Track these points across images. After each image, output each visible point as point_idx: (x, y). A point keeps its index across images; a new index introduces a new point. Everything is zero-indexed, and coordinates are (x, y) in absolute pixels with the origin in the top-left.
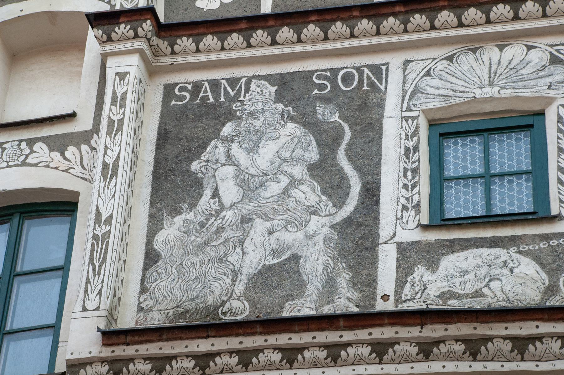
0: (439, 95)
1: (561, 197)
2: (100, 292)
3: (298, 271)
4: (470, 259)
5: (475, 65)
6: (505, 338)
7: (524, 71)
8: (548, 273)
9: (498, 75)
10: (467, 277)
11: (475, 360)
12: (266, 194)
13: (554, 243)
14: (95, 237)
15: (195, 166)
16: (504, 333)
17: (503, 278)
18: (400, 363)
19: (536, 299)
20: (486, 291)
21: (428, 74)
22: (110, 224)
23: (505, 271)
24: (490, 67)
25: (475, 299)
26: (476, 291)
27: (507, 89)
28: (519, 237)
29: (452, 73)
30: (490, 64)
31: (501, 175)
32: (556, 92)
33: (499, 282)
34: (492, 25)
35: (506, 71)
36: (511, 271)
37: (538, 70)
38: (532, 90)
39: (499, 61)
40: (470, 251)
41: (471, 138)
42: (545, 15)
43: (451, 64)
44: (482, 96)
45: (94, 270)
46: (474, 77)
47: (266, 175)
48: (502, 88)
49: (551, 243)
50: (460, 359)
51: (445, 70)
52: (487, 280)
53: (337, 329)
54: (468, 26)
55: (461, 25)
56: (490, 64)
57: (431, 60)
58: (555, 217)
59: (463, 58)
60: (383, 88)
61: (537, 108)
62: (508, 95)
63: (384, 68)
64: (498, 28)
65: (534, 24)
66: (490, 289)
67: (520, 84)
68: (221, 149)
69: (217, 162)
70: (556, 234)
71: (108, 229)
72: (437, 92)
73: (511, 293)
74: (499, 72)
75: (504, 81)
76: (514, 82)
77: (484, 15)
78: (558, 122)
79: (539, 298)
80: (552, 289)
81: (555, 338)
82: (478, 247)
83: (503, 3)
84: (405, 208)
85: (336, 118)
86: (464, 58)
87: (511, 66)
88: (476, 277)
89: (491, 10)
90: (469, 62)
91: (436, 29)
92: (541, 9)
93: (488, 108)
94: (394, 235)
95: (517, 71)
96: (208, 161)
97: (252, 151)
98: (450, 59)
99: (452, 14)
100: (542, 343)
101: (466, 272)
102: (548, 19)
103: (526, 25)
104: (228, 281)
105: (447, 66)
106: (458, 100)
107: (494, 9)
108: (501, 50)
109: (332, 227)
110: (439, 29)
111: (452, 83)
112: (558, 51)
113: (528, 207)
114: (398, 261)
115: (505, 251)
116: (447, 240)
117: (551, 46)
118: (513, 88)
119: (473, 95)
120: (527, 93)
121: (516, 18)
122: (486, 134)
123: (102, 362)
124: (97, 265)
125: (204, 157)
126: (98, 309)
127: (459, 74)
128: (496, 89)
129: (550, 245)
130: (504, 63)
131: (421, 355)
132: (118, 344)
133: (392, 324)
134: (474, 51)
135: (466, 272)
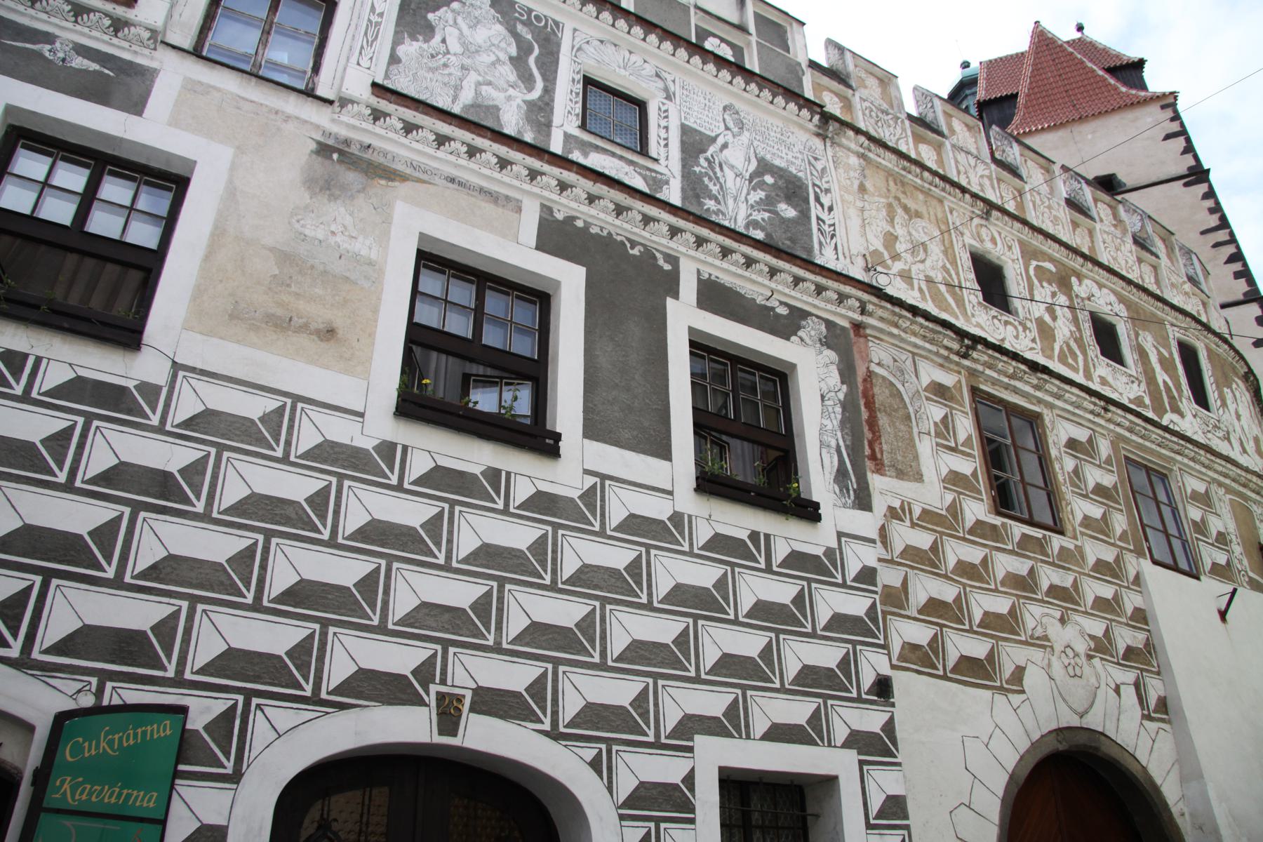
2: (371, 58)
3: (498, 117)
7: (642, 72)
11: (617, 218)
12: (481, 59)
13: (654, 174)
14: (369, 20)
15: (430, 16)
16: (641, 208)
18: (572, 200)
21: (588, 42)
22: (382, 17)
45: (368, 42)
47: (479, 47)
50: (609, 214)
53: (541, 160)
60: (560, 36)
63: (561, 25)
68: (450, 16)
69: (447, 22)
71: (380, 20)
84: (569, 112)
85: (529, 37)
94: (562, 125)
96: (440, 18)
97: (471, 27)
98: (602, 42)
104: (450, 100)
109: (524, 102)
114: (564, 142)
123: (367, 106)
124: (370, 40)
125: (437, 13)
126: (369, 69)
128: (627, 73)
131: (587, 201)
132: (384, 99)
133: (577, 173)
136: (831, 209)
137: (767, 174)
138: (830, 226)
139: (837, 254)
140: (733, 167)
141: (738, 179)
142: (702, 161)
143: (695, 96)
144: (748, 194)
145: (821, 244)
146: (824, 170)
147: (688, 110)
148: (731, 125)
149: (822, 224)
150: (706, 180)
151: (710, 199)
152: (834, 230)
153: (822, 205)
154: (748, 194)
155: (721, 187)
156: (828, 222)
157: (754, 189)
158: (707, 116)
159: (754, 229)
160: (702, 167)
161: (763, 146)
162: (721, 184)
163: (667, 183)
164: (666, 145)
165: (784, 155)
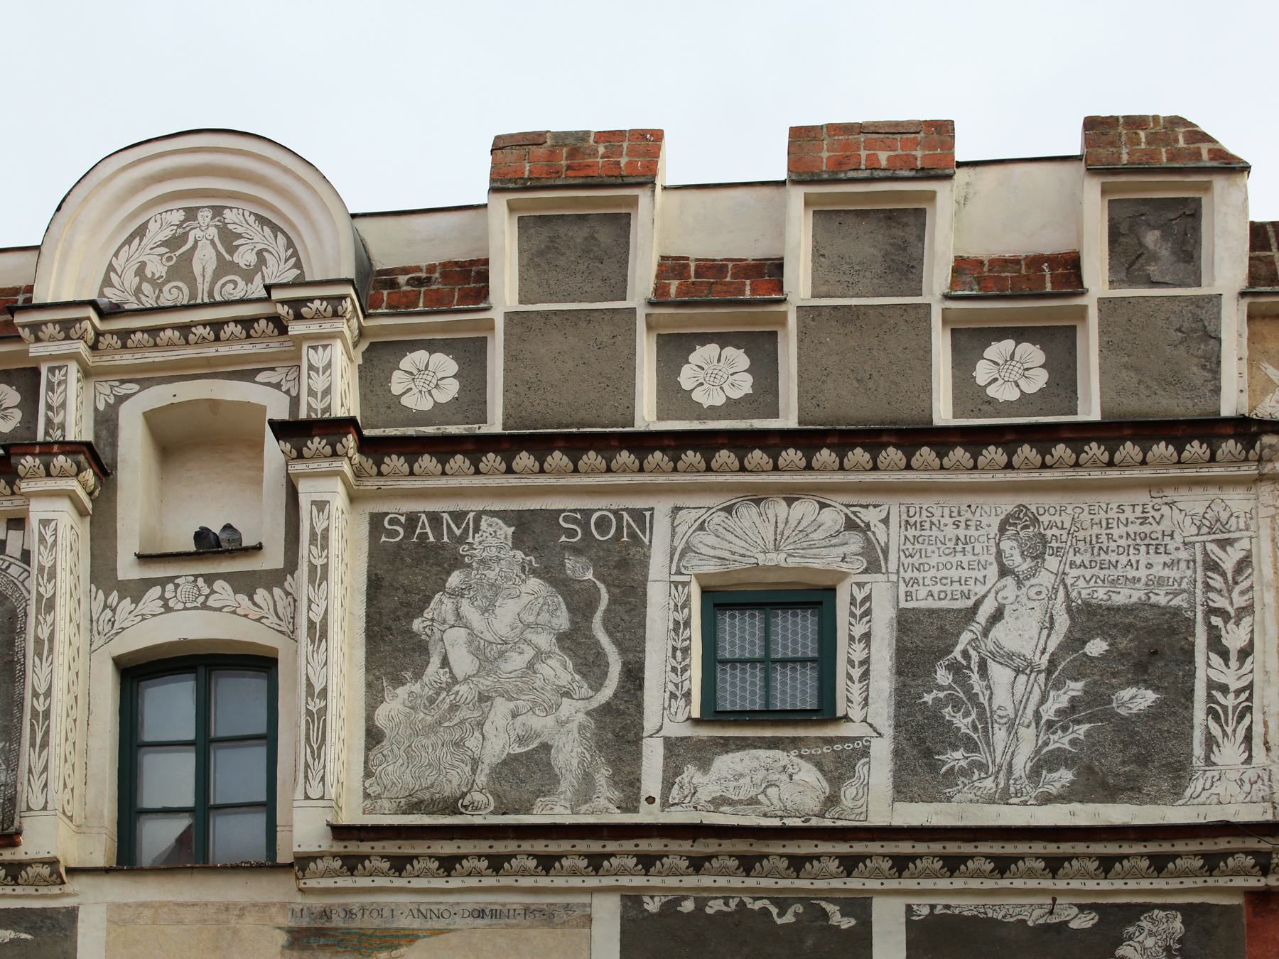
0: (715, 557)
1: (849, 695)
4: (746, 761)
5: (758, 521)
6: (781, 856)
8: (830, 781)
9: (785, 538)
10: (742, 781)
13: (838, 747)
17: (781, 785)
19: (815, 809)
20: (761, 798)
23: (784, 777)
24: (776, 527)
25: (749, 807)
26: (751, 798)
27: (795, 557)
28: (800, 739)
29: (731, 530)
30: (777, 522)
31: (784, 662)
32: (851, 566)
33: (777, 789)
34: (780, 473)
35: (794, 533)
36: (791, 777)
37: (831, 536)
38: (823, 561)
39: (787, 518)
40: (747, 751)
41: (751, 612)
42: (842, 468)
43: (730, 517)
44: (766, 563)
46: (757, 537)
48: (789, 555)
49: (835, 748)
51: (722, 524)
52: (764, 786)
54: (751, 471)
55: (743, 469)
56: (777, 522)
57: (705, 510)
58: (840, 718)
59: (743, 511)
61: (827, 582)
62: (796, 565)
64: (786, 478)
65: (828, 477)
66: (766, 796)
67: (811, 551)
70: (841, 737)
72: (712, 553)
73: (789, 801)
74: (786, 534)
75: (792, 547)
76: (803, 549)
77: (771, 460)
78: (851, 604)
79: (818, 808)
80: (832, 800)
81: (833, 858)
82: (755, 747)
83: (794, 448)
86: (745, 510)
87: (800, 528)
88: (752, 781)
89: (779, 455)
90: (751, 518)
91: (712, 471)
92: (838, 460)
93: (772, 578)
95: (807, 535)
99: (732, 455)
100: (820, 862)
101: (741, 775)
102: (845, 473)
103: (820, 477)
105: (725, 520)
106: (737, 566)
107: (784, 453)
108: (789, 506)
110: (716, 471)
111: (730, 542)
112: (854, 513)
113: (810, 703)
115: (785, 754)
116: (721, 738)
117: (847, 506)
118: (802, 557)
119: (755, 561)
120: (818, 564)
121: (809, 467)
122: (768, 609)
127: (739, 532)
128: (783, 556)
129: (833, 750)
130: (793, 523)
134: (757, 502)
135: (741, 775)
136: (1245, 653)
137: (1093, 638)
138: (1238, 692)
139: (1250, 750)
140: (1011, 656)
141: (1022, 678)
142: (943, 676)
143: (935, 532)
144: (1043, 700)
145: (1210, 741)
146: (1244, 563)
147: (916, 574)
148: (1015, 559)
149: (1218, 695)
150: (947, 712)
151: (955, 748)
152: (1250, 698)
153: (1224, 654)
154: (1043, 700)
155: (982, 714)
156: (1234, 685)
157: (1058, 685)
158: (960, 566)
159: (1050, 771)
160: (941, 688)
161: (1088, 573)
162: (979, 706)
163: (865, 753)
164: (865, 675)
165: (1142, 573)
